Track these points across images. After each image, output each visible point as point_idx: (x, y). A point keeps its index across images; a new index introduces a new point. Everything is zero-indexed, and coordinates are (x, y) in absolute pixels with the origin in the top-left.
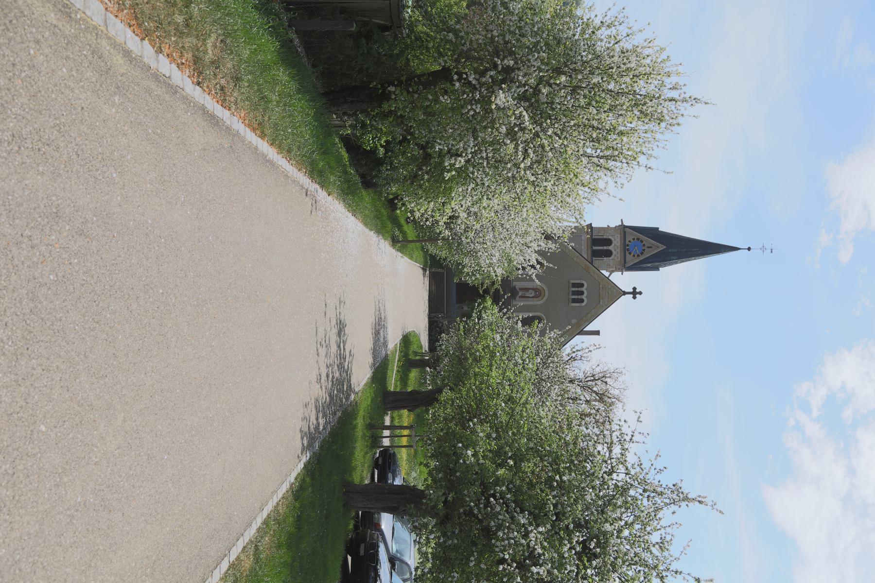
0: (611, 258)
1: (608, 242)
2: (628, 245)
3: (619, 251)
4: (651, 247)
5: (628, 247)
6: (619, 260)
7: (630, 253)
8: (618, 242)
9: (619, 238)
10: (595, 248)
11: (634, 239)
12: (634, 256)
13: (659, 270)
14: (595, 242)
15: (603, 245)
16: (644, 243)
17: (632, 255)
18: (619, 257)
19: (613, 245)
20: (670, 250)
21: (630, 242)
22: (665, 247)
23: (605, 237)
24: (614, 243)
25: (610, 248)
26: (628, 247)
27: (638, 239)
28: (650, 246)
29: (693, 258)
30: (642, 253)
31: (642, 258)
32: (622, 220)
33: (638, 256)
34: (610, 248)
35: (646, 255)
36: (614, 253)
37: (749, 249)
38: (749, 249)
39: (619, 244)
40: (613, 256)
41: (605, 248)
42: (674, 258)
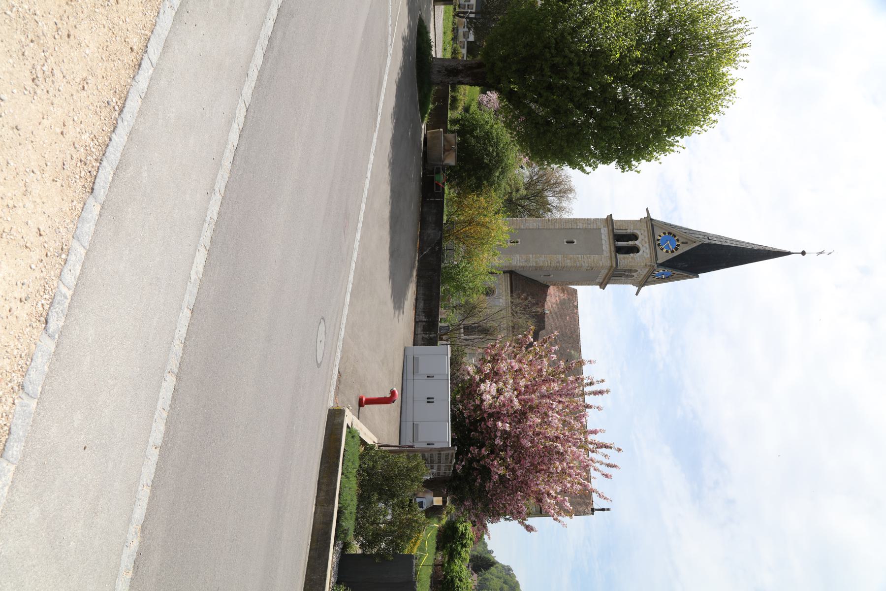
0: (638, 254)
1: (634, 237)
2: (658, 240)
3: (648, 246)
4: (687, 243)
5: (659, 242)
11: (664, 233)
12: (667, 252)
13: (698, 277)
14: (618, 237)
15: (627, 242)
17: (665, 250)
18: (649, 253)
19: (640, 239)
21: (660, 236)
23: (629, 231)
26: (659, 242)
27: (670, 233)
28: (684, 241)
30: (677, 249)
31: (676, 254)
32: (647, 209)
33: (672, 252)
34: (637, 242)
37: (803, 253)
38: (803, 253)
41: (630, 243)
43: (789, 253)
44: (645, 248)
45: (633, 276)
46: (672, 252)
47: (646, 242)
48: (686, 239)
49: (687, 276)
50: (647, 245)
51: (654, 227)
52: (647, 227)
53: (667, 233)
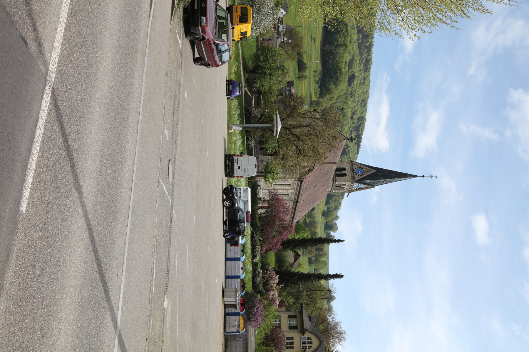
1: (344, 169)
2: (355, 170)
3: (350, 174)
4: (368, 171)
5: (355, 172)
6: (351, 177)
7: (356, 174)
8: (349, 169)
9: (350, 167)
10: (337, 172)
11: (358, 168)
12: (359, 176)
16: (364, 169)
17: (358, 175)
19: (347, 170)
20: (379, 174)
21: (355, 169)
22: (375, 171)
23: (342, 167)
24: (347, 169)
25: (345, 172)
26: (355, 172)
27: (360, 168)
28: (367, 171)
29: (392, 179)
30: (363, 174)
31: (363, 176)
33: (361, 176)
34: (345, 172)
35: (365, 175)
36: (348, 174)
37: (423, 176)
38: (423, 176)
39: (350, 170)
40: (347, 176)
41: (342, 172)
42: (382, 178)
43: (417, 176)
44: (349, 174)
45: (344, 188)
46: (361, 176)
47: (349, 172)
48: (368, 170)
49: (369, 187)
50: (350, 173)
51: (354, 165)
52: (350, 165)
53: (359, 167)
